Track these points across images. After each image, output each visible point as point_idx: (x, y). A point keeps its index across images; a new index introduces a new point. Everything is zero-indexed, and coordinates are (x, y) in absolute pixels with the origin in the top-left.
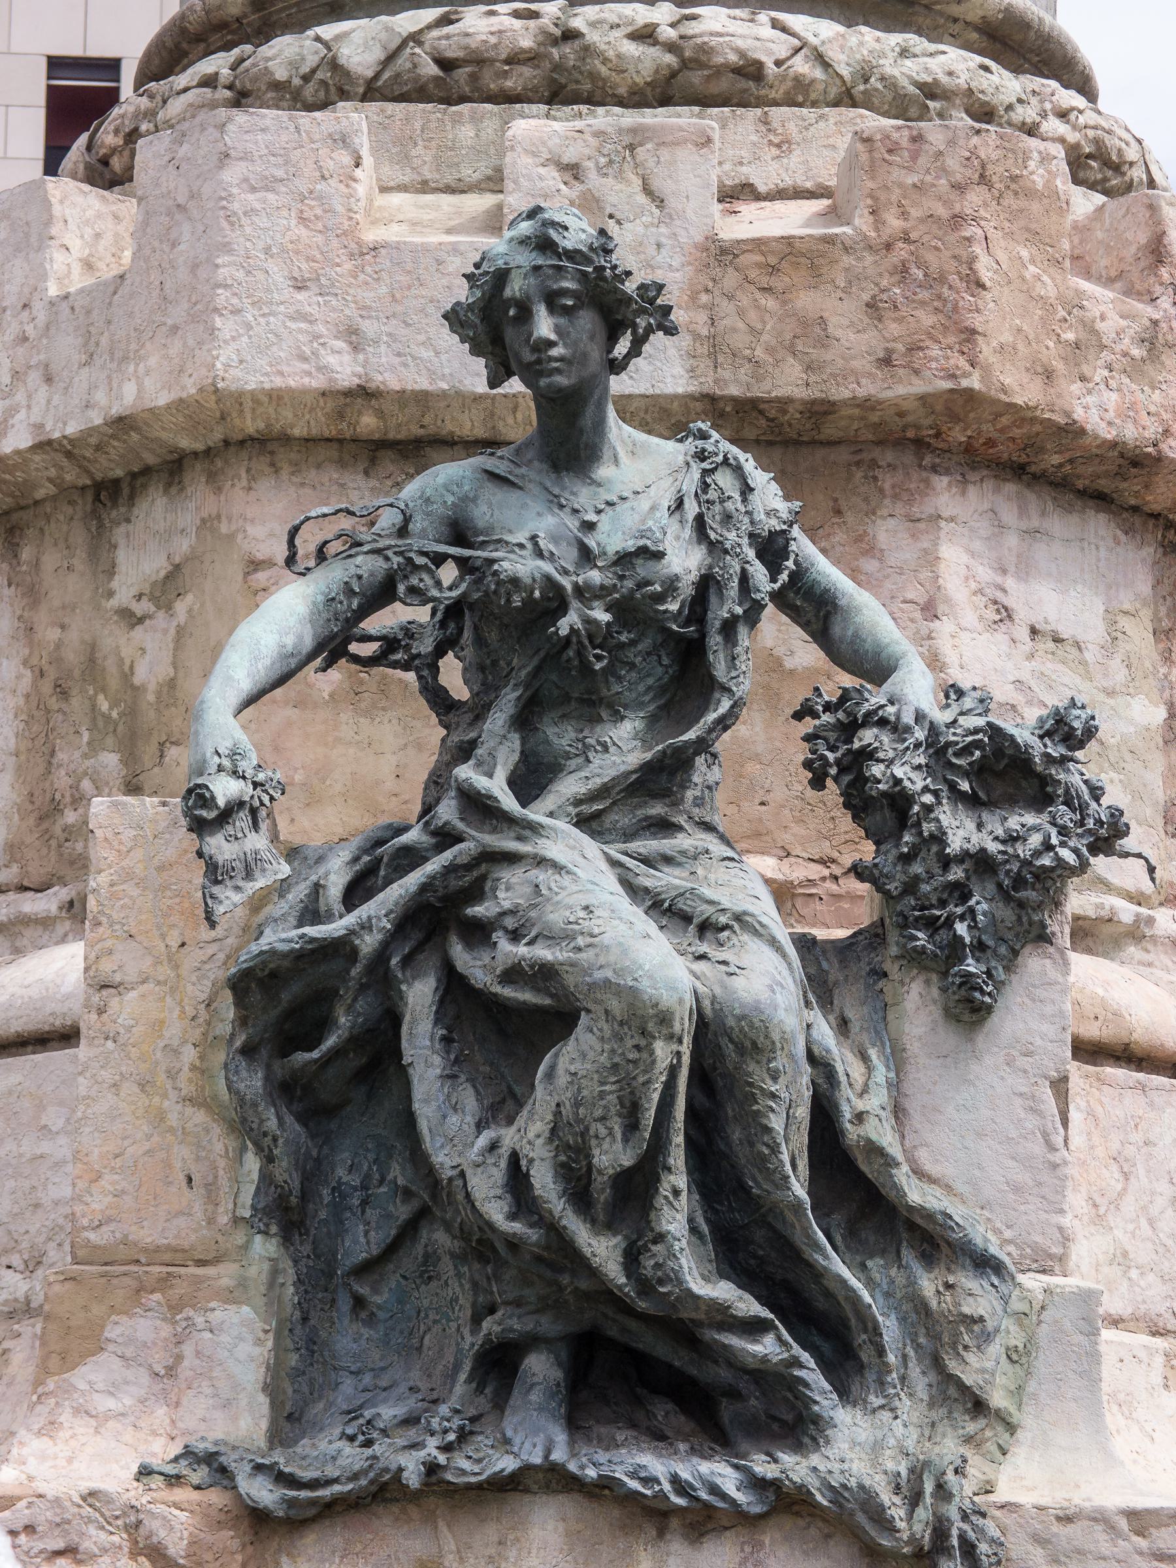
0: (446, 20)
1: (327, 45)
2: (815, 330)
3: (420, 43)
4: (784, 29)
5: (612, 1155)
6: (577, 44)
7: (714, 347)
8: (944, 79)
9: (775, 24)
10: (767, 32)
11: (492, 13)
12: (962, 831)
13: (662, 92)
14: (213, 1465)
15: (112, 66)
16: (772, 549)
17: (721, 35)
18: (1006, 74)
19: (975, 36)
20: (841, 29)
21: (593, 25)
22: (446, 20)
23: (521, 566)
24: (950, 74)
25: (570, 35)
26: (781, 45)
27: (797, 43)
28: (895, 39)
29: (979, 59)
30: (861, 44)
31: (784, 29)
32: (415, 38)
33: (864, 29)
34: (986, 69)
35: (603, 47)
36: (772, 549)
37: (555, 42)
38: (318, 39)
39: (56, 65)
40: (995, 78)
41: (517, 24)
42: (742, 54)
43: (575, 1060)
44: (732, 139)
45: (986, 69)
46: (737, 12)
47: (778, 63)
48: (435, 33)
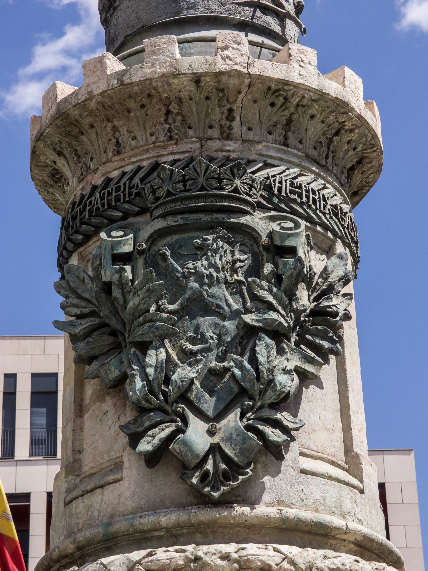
0: (150, 555)
1: (105, 566)
3: (141, 564)
4: (279, 551)
6: (200, 562)
8: (341, 567)
9: (275, 550)
10: (272, 553)
11: (167, 551)
17: (253, 555)
18: (365, 562)
19: (352, 546)
20: (300, 550)
21: (205, 554)
22: (150, 555)
24: (343, 565)
25: (197, 559)
26: (278, 558)
27: (283, 556)
28: (321, 552)
29: (354, 557)
30: (308, 555)
31: (279, 551)
32: (139, 562)
33: (309, 549)
34: (357, 561)
35: (210, 562)
37: (191, 561)
38: (102, 564)
40: (361, 565)
41: (177, 555)
42: (262, 561)
45: (357, 561)
46: (260, 545)
47: (277, 565)
48: (146, 560)
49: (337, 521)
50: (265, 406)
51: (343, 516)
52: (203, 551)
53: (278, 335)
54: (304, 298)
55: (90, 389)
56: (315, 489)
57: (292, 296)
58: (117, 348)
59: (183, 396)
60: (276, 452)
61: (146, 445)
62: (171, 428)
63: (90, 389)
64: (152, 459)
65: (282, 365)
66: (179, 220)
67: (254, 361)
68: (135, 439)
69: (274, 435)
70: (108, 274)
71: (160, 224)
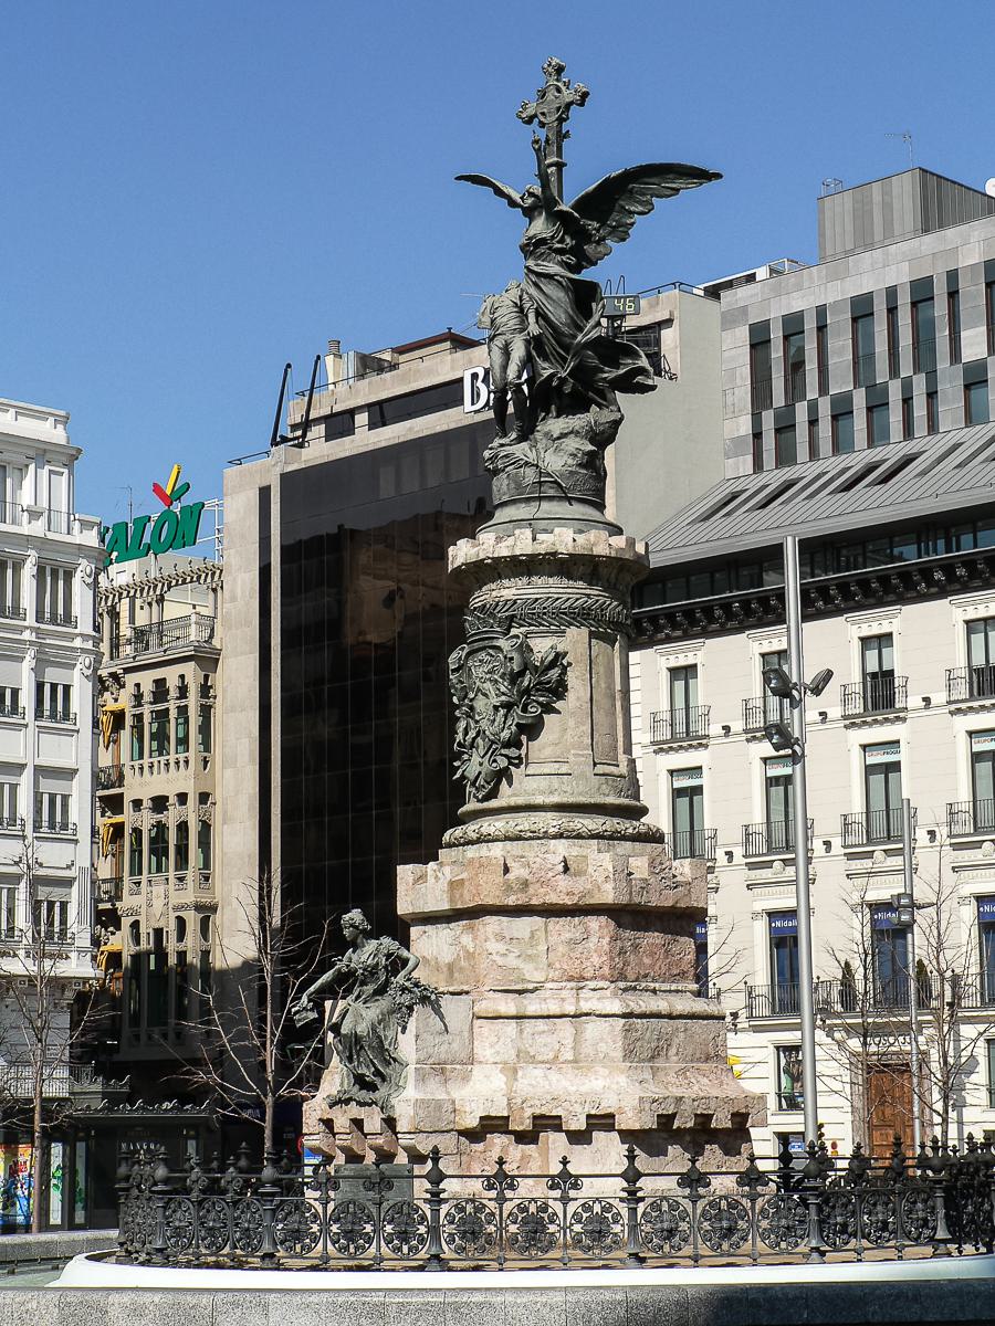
7: (452, 900)
49: (539, 800)
56: (532, 784)
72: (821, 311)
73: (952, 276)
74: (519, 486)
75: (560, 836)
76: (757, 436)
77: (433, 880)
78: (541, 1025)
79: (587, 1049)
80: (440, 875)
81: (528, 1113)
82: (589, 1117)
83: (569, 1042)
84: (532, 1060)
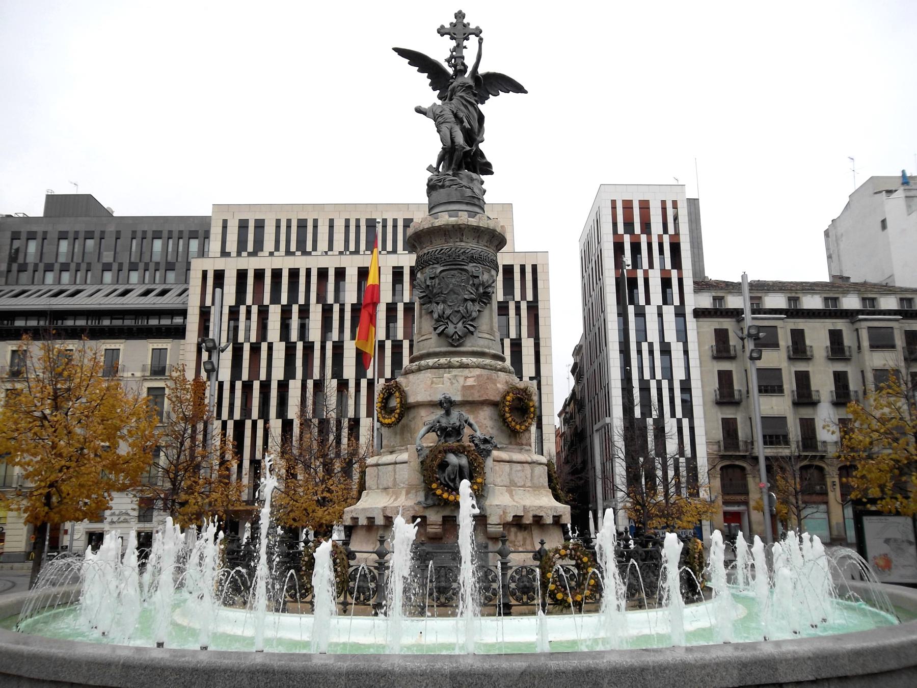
2: (473, 394)
5: (452, 477)
7: (463, 396)
12: (482, 447)
13: (459, 367)
14: (419, 503)
15: (402, 267)
16: (466, 421)
23: (444, 425)
36: (466, 421)
39: (394, 268)
43: (449, 468)
44: (466, 372)
49: (487, 350)
50: (469, 319)
51: (489, 348)
52: (452, 360)
53: (473, 301)
54: (481, 290)
55: (423, 312)
56: (481, 342)
57: (477, 289)
58: (430, 302)
59: (448, 318)
60: (472, 333)
61: (439, 331)
62: (443, 327)
63: (423, 312)
64: (439, 335)
65: (474, 308)
66: (448, 267)
67: (466, 308)
68: (435, 329)
69: (471, 329)
70: (428, 283)
71: (442, 268)
72: (45, 233)
73: (103, 232)
74: (462, 196)
75: (500, 370)
76: (9, 271)
77: (449, 384)
78: (519, 467)
79: (536, 481)
80: (454, 381)
81: (531, 514)
82: (554, 517)
83: (529, 476)
84: (515, 485)
